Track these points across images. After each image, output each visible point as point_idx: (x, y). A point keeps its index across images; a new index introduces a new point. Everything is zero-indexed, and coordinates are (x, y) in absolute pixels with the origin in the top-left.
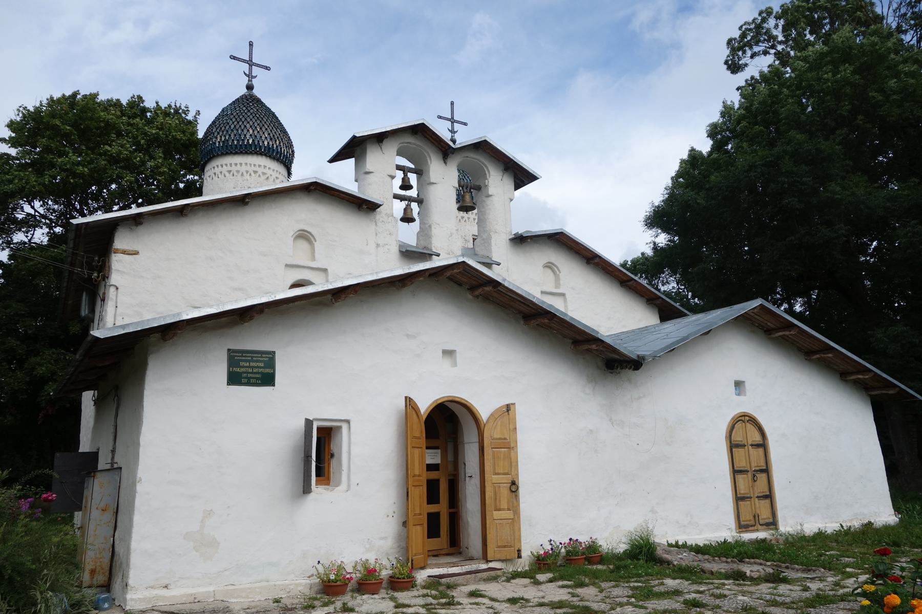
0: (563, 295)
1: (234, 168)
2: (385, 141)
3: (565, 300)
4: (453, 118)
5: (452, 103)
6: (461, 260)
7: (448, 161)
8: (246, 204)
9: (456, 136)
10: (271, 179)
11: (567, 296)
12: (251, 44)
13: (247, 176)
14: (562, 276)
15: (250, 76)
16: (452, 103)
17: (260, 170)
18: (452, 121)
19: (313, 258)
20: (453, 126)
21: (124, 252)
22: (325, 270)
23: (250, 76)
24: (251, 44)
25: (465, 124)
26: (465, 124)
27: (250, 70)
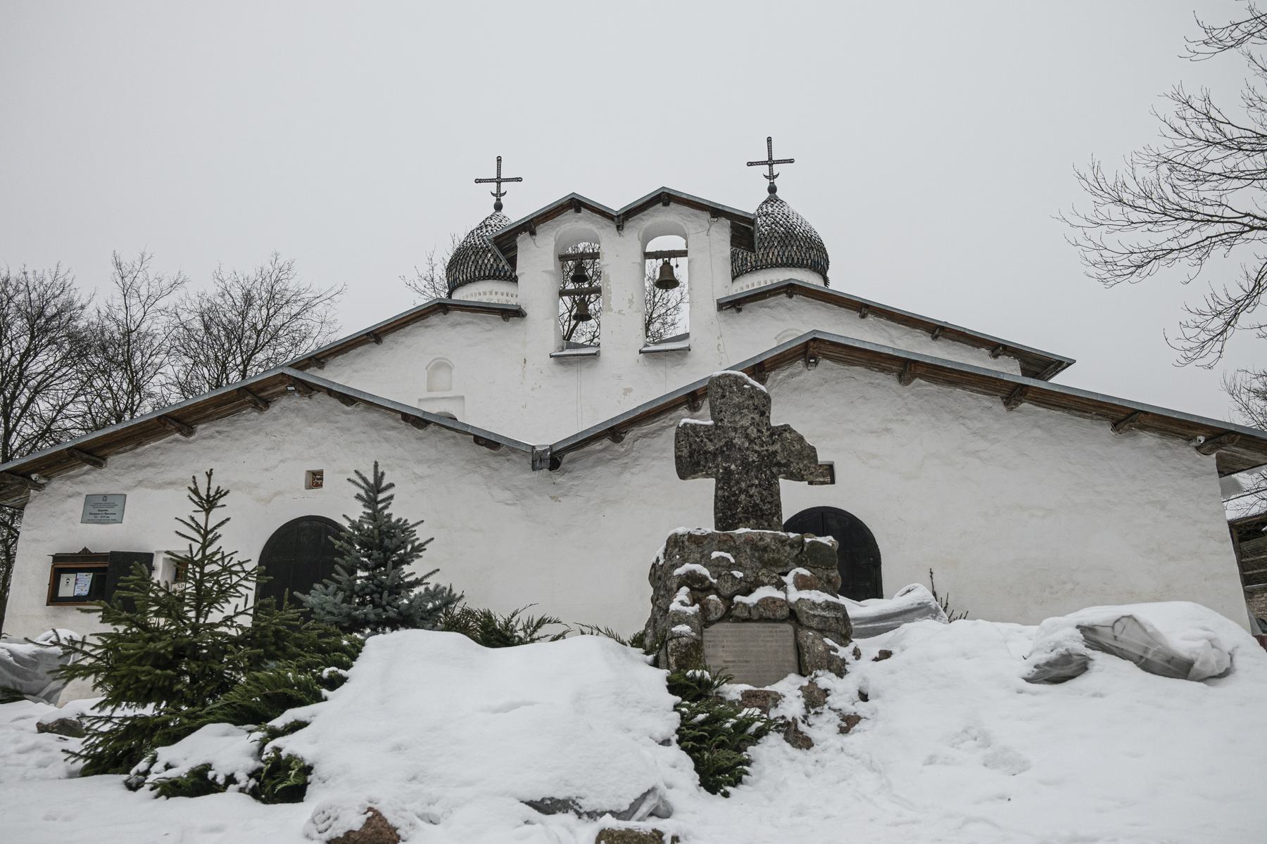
4: (770, 159)
5: (769, 140)
12: (499, 160)
15: (499, 195)
16: (769, 140)
18: (770, 162)
20: (771, 170)
22: (463, 398)
23: (499, 195)
24: (499, 160)
25: (791, 161)
26: (791, 161)
27: (499, 188)
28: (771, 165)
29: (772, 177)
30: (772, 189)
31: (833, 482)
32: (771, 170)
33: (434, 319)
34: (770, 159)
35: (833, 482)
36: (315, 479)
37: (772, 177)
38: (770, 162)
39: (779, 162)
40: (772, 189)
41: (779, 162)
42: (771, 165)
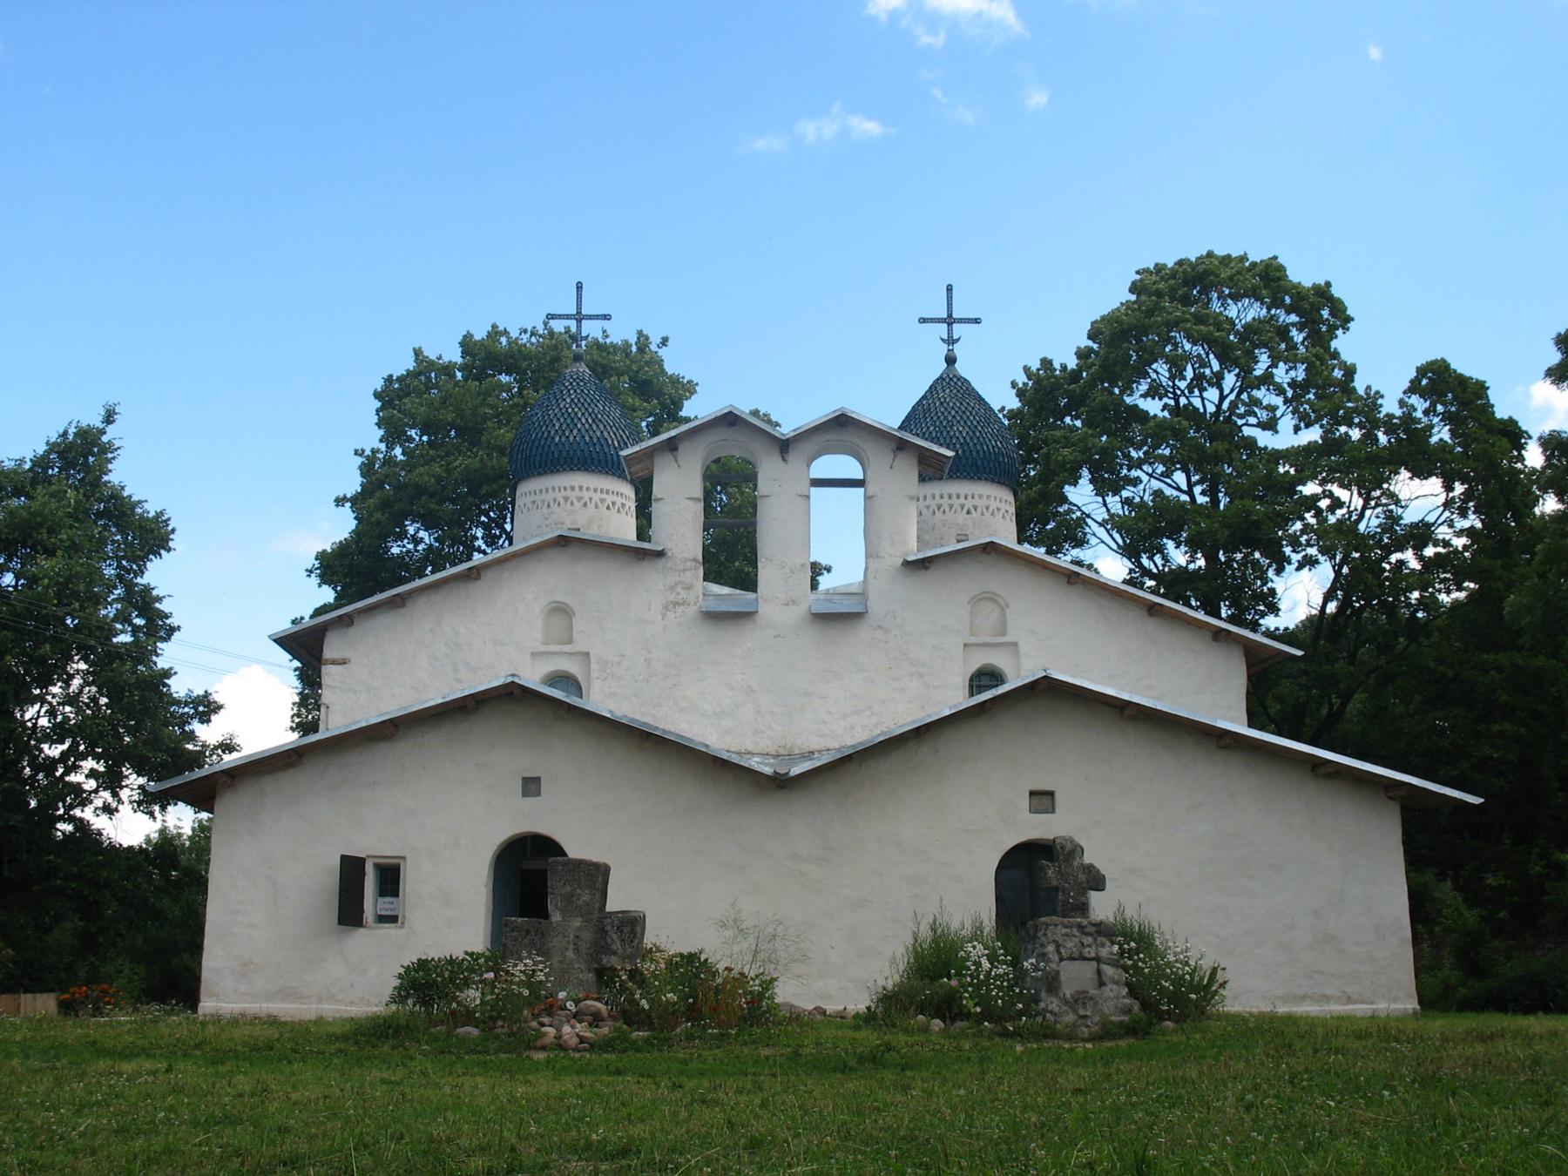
0: (1015, 644)
1: (538, 498)
2: (682, 448)
3: (1017, 653)
4: (950, 315)
5: (949, 289)
6: (509, 680)
7: (791, 457)
8: (478, 578)
9: (957, 348)
10: (591, 506)
11: (1023, 649)
12: (579, 287)
13: (554, 507)
14: (1010, 614)
16: (949, 289)
17: (572, 495)
18: (950, 321)
19: (570, 641)
20: (950, 331)
21: (334, 662)
24: (579, 287)
25: (977, 321)
26: (977, 321)
28: (950, 325)
29: (951, 341)
30: (951, 360)
31: (1053, 811)
32: (950, 331)
33: (550, 553)
34: (950, 315)
35: (1053, 811)
36: (531, 786)
37: (951, 341)
38: (950, 321)
39: (961, 321)
40: (951, 360)
41: (961, 321)
42: (950, 325)
